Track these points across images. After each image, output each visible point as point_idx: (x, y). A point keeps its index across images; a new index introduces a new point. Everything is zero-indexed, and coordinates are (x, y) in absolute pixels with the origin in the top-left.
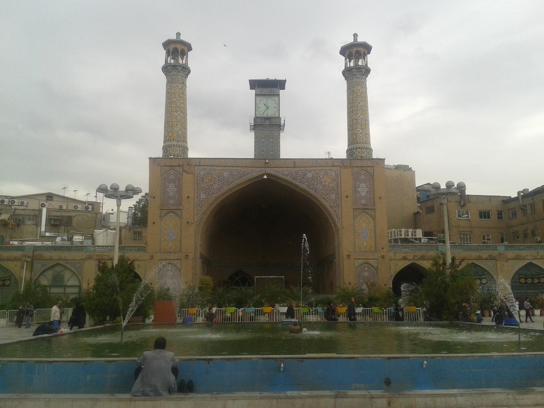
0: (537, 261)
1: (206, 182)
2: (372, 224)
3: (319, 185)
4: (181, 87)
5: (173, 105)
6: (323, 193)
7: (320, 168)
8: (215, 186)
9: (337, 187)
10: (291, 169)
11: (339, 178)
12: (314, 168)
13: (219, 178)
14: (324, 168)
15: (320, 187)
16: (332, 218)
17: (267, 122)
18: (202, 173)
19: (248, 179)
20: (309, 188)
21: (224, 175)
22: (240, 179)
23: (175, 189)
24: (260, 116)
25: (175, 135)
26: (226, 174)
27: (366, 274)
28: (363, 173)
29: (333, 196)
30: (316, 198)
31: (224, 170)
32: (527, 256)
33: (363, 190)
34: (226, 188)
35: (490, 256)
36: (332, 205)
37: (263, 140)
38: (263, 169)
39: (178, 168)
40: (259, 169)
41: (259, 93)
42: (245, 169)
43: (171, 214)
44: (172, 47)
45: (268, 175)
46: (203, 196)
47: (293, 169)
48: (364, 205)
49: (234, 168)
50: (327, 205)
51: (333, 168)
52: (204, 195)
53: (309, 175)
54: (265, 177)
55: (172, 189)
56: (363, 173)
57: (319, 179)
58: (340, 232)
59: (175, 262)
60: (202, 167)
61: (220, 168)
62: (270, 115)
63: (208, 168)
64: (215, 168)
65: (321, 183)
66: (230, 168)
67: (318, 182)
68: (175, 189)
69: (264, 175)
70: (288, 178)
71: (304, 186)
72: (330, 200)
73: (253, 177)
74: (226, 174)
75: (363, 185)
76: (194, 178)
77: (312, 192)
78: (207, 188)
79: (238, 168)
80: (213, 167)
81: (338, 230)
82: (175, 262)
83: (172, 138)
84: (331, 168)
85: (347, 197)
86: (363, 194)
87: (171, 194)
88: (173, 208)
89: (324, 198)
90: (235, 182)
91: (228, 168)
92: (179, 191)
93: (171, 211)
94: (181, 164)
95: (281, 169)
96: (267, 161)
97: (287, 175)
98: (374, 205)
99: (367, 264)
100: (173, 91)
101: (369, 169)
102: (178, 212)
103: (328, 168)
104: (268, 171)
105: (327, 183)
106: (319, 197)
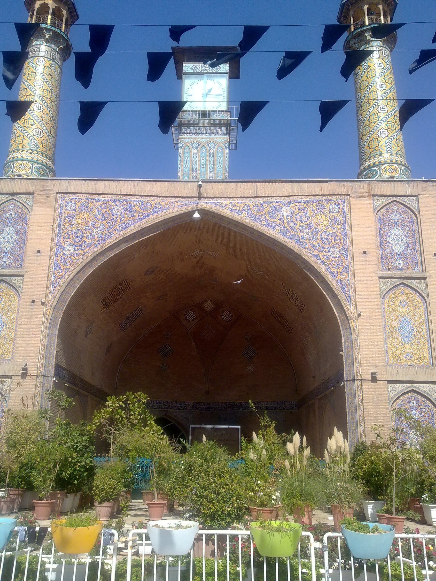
1: (78, 223)
2: (422, 308)
3: (306, 231)
4: (47, 65)
6: (314, 246)
7: (308, 198)
8: (97, 232)
9: (344, 234)
10: (248, 200)
11: (348, 217)
12: (295, 199)
13: (103, 215)
14: (317, 198)
15: (307, 234)
16: (335, 296)
19: (162, 219)
20: (284, 234)
21: (115, 211)
22: (147, 219)
23: (15, 237)
26: (118, 209)
28: (395, 208)
29: (335, 252)
30: (298, 256)
31: (115, 201)
33: (398, 240)
34: (117, 236)
36: (333, 270)
37: (195, 151)
38: (194, 200)
39: (24, 197)
40: (184, 201)
41: (191, 71)
42: (158, 200)
45: (201, 211)
46: (69, 250)
47: (253, 200)
48: (401, 270)
49: (134, 198)
50: (323, 270)
51: (334, 198)
52: (72, 248)
53: (286, 211)
54: (197, 215)
56: (395, 208)
57: (305, 219)
58: (352, 324)
60: (72, 196)
63: (83, 197)
64: (97, 197)
65: (309, 226)
66: (126, 198)
67: (304, 224)
68: (15, 237)
69: (193, 212)
70: (243, 218)
72: (328, 259)
73: (171, 215)
74: (118, 209)
77: (291, 244)
78: (80, 234)
79: (143, 199)
80: (92, 197)
81: (347, 319)
83: (20, 147)
84: (330, 197)
85: (365, 253)
86: (399, 248)
88: (6, 272)
89: (315, 256)
90: (137, 224)
91: (123, 198)
92: (22, 241)
94: (31, 190)
95: (229, 201)
96: (200, 183)
97: (238, 212)
98: (423, 269)
99: (414, 394)
101: (407, 199)
102: (14, 280)
103: (323, 198)
104: (205, 204)
106: (306, 253)
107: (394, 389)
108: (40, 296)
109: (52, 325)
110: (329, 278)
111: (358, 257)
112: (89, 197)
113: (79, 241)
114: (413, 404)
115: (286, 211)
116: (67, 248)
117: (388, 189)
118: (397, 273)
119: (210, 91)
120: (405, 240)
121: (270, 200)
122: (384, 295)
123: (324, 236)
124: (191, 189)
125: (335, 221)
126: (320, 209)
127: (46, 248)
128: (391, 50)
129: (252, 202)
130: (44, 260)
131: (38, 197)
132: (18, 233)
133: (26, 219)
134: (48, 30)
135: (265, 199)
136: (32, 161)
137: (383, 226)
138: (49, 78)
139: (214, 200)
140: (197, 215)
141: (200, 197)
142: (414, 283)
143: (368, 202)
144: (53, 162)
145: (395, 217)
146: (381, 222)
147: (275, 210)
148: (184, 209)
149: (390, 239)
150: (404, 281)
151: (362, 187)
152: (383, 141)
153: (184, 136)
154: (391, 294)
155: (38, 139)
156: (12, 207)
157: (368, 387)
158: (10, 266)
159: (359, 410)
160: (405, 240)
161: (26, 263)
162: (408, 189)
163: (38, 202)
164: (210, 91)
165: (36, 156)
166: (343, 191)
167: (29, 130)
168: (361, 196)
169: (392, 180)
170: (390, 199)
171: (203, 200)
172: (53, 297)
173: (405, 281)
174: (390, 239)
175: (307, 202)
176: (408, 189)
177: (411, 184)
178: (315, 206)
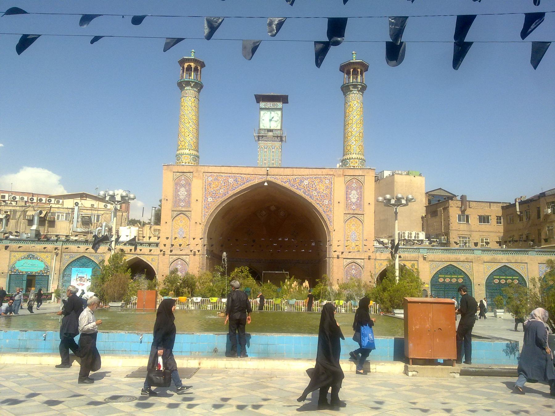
0: (511, 264)
2: (361, 227)
4: (193, 101)
5: (186, 117)
6: (317, 199)
8: (222, 191)
9: (331, 193)
15: (315, 193)
16: (325, 222)
17: (271, 134)
18: (210, 179)
23: (186, 193)
24: (263, 128)
25: (187, 144)
26: (231, 180)
27: (353, 272)
30: (310, 203)
32: (502, 259)
33: (354, 196)
34: (231, 193)
35: (466, 258)
38: (265, 176)
40: (261, 176)
41: (264, 107)
42: (248, 176)
43: (182, 215)
44: (186, 65)
45: (268, 182)
46: (210, 199)
49: (238, 175)
51: (327, 176)
53: (306, 182)
54: (266, 184)
55: (183, 192)
57: (314, 186)
59: (184, 257)
60: (211, 174)
61: (226, 175)
62: (272, 128)
63: (215, 174)
64: (221, 174)
68: (186, 193)
69: (264, 182)
70: (287, 185)
71: (300, 193)
74: (231, 180)
75: (354, 192)
76: (203, 183)
77: (308, 198)
78: (214, 192)
79: (242, 176)
81: (329, 232)
82: (184, 257)
86: (354, 200)
87: (182, 197)
88: (183, 209)
91: (233, 175)
92: (189, 195)
93: (181, 212)
94: (191, 171)
96: (268, 169)
97: (285, 182)
100: (186, 104)
103: (323, 177)
104: (269, 178)
105: (321, 190)
106: (314, 203)
107: (346, 261)
108: (199, 221)
109: (205, 233)
110: (323, 214)
111: (336, 204)
112: (218, 174)
113: (214, 195)
114: (354, 267)
115: (306, 182)
116: (209, 199)
117: (351, 172)
118: (352, 212)
119: (273, 118)
120: (357, 196)
121: (299, 177)
122: (345, 222)
123: (322, 194)
124: (263, 171)
125: (327, 187)
126: (321, 181)
127: (200, 199)
128: (362, 95)
129: (291, 178)
130: (199, 204)
131: (195, 174)
132: (187, 191)
133: (190, 185)
134: (193, 82)
135: (297, 177)
136: (190, 155)
137: (348, 188)
138: (194, 108)
139: (274, 176)
140: (266, 184)
141: (268, 175)
142: (359, 216)
143: (342, 179)
144: (198, 151)
145: (354, 185)
146: (347, 188)
147: (301, 182)
148: (260, 181)
149: (350, 196)
150: (354, 215)
151: (341, 172)
152: (353, 147)
153: (260, 142)
154: (349, 221)
155: (192, 142)
156: (183, 178)
157: (335, 260)
158: (184, 206)
159: (331, 270)
160: (357, 196)
161: (192, 205)
162: (360, 172)
163: (195, 177)
164: (273, 118)
165: (192, 152)
166: (332, 173)
167: (187, 138)
168: (339, 176)
169: (354, 168)
170: (352, 177)
171: (269, 176)
172: (204, 221)
173: (355, 215)
174: (350, 196)
175: (315, 178)
176: (360, 172)
177: (362, 170)
178: (319, 180)
